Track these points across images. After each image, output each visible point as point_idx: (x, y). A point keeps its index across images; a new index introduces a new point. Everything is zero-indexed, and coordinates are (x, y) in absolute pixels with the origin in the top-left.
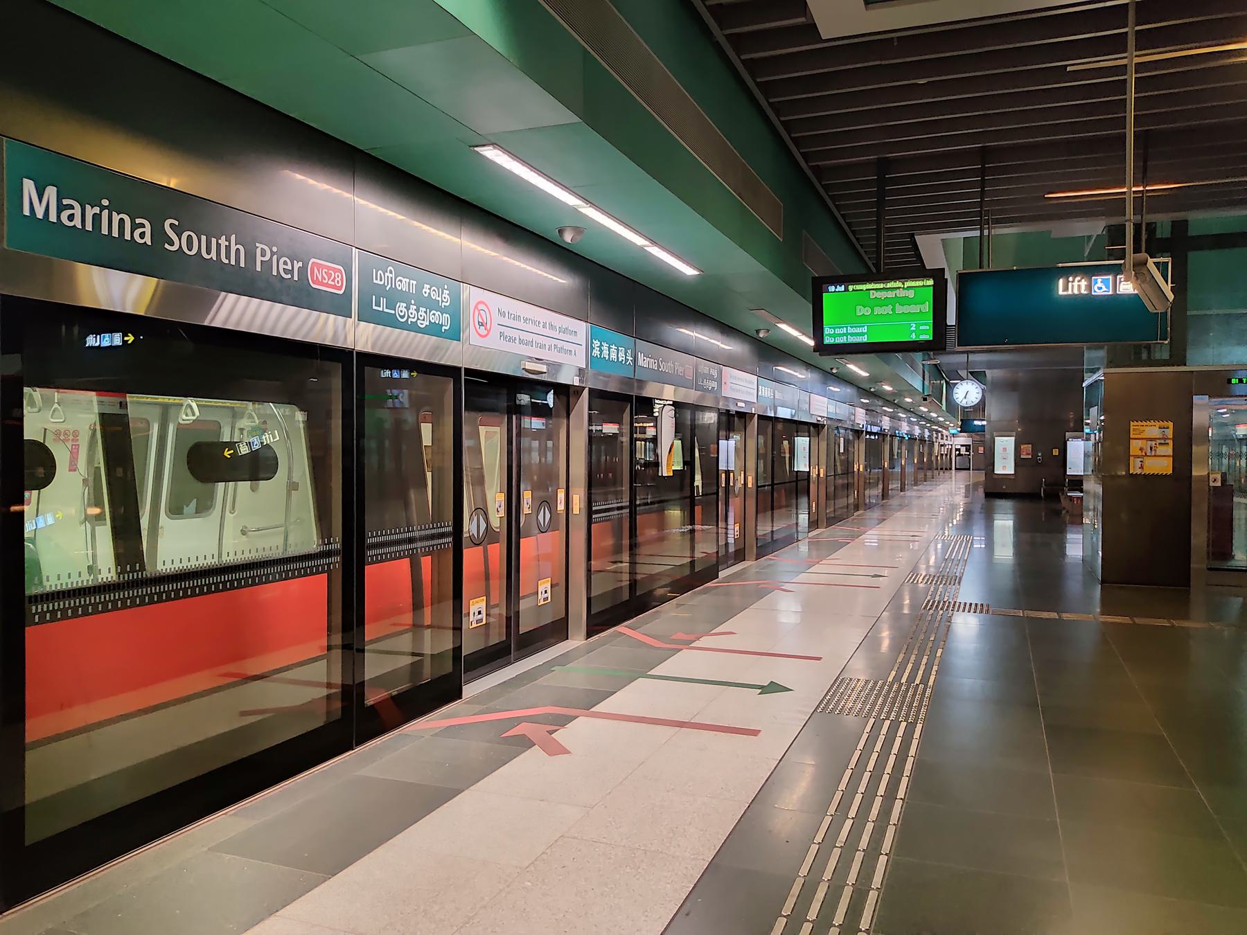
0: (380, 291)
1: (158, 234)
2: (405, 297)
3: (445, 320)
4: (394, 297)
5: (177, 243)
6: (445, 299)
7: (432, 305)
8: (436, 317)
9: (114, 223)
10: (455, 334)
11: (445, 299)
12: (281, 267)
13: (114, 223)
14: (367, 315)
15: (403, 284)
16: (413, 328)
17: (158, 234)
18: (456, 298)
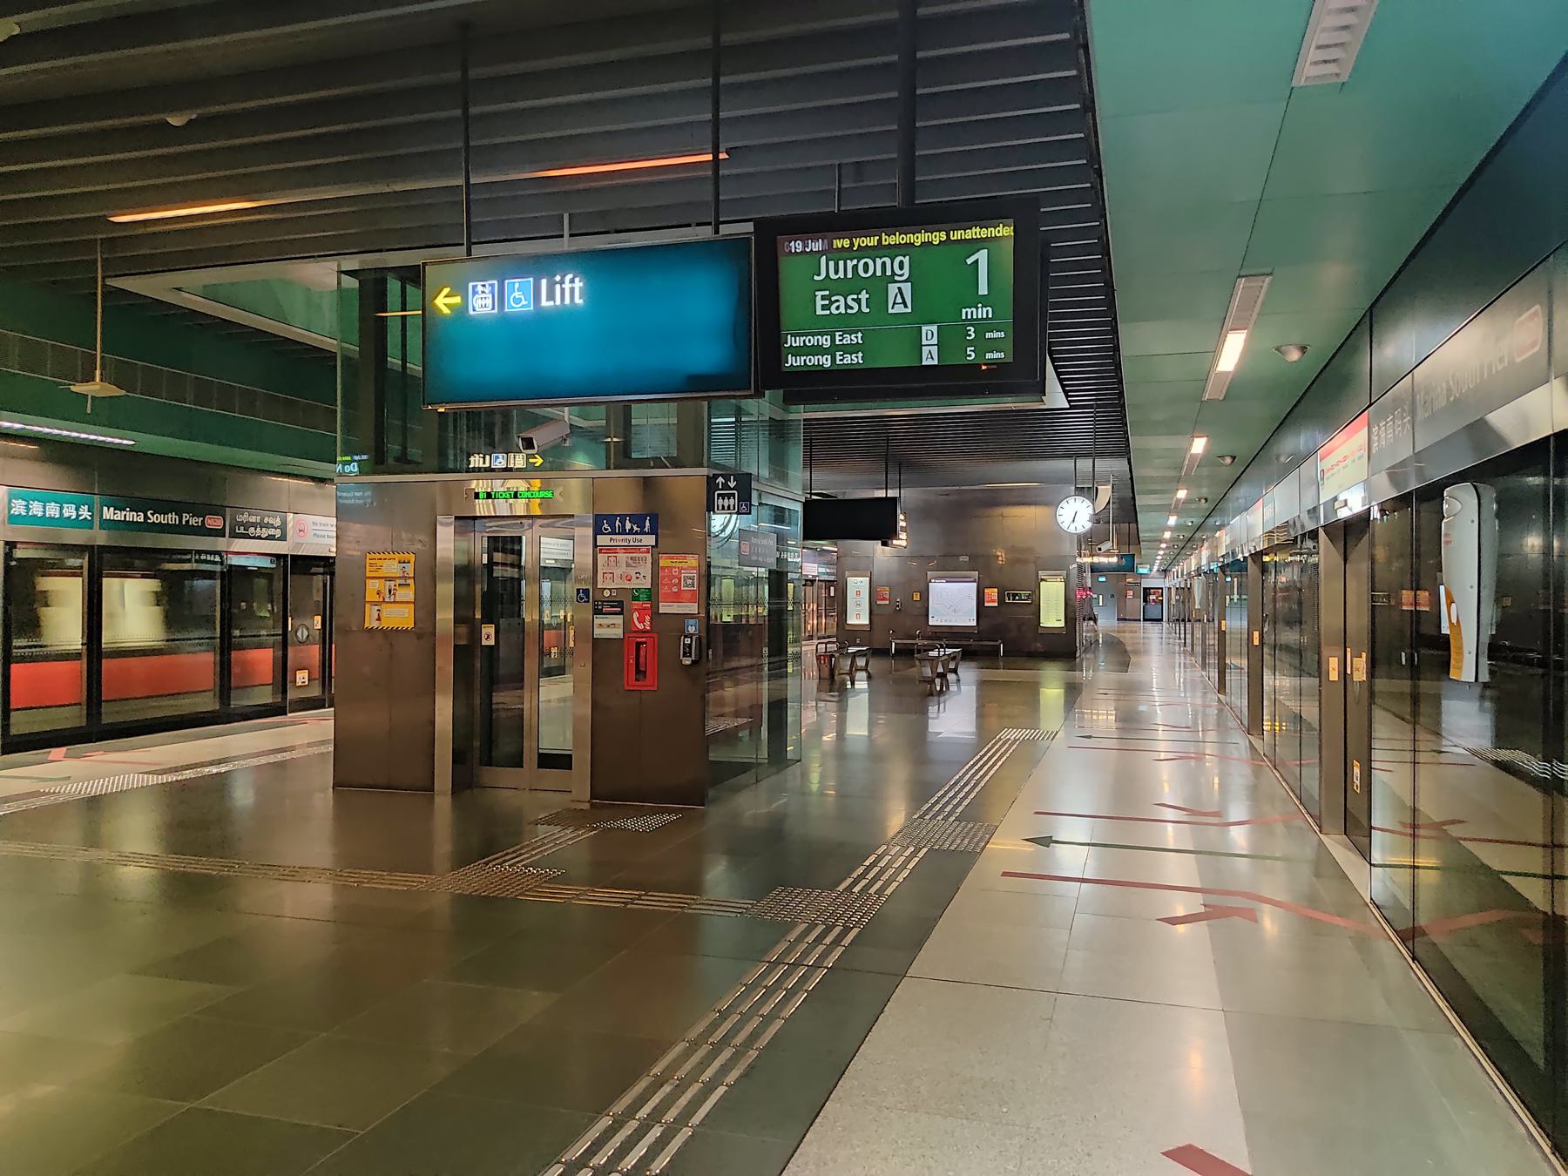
0: (241, 524)
1: (146, 517)
2: (254, 525)
3: (278, 533)
4: (247, 525)
5: (153, 519)
6: (278, 522)
7: (272, 526)
8: (272, 531)
9: (131, 516)
10: (283, 538)
11: (278, 522)
12: (193, 522)
13: (131, 516)
14: (234, 535)
15: (253, 519)
16: (260, 538)
17: (146, 517)
18: (284, 523)
